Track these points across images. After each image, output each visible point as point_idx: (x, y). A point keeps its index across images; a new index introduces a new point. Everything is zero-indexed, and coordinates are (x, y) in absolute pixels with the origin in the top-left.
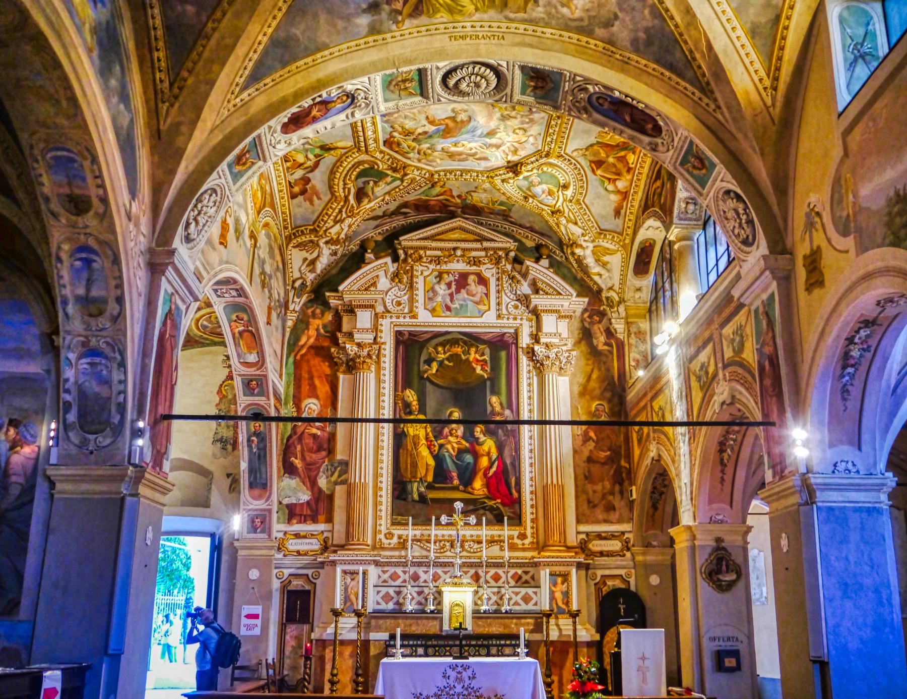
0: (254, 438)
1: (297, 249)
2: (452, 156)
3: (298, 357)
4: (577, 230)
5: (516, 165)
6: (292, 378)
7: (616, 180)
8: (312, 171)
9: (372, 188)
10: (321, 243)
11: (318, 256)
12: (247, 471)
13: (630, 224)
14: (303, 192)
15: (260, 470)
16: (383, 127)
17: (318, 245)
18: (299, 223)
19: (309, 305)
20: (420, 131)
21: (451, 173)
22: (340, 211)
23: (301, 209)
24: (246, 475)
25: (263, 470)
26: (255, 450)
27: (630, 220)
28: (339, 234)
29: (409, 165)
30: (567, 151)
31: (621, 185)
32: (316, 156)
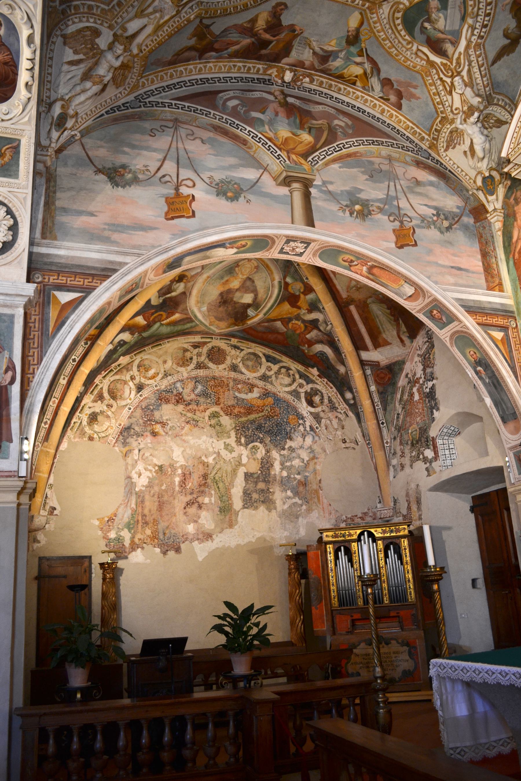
0: (479, 368)
1: (450, 149)
3: (517, 256)
6: (518, 282)
8: (379, 71)
9: (435, 29)
10: (458, 124)
11: (472, 140)
12: (493, 406)
14: (400, 95)
15: (502, 400)
17: (462, 131)
18: (428, 124)
19: (510, 194)
22: (441, 79)
24: (495, 410)
25: (505, 398)
26: (487, 381)
28: (463, 102)
32: (360, 54)
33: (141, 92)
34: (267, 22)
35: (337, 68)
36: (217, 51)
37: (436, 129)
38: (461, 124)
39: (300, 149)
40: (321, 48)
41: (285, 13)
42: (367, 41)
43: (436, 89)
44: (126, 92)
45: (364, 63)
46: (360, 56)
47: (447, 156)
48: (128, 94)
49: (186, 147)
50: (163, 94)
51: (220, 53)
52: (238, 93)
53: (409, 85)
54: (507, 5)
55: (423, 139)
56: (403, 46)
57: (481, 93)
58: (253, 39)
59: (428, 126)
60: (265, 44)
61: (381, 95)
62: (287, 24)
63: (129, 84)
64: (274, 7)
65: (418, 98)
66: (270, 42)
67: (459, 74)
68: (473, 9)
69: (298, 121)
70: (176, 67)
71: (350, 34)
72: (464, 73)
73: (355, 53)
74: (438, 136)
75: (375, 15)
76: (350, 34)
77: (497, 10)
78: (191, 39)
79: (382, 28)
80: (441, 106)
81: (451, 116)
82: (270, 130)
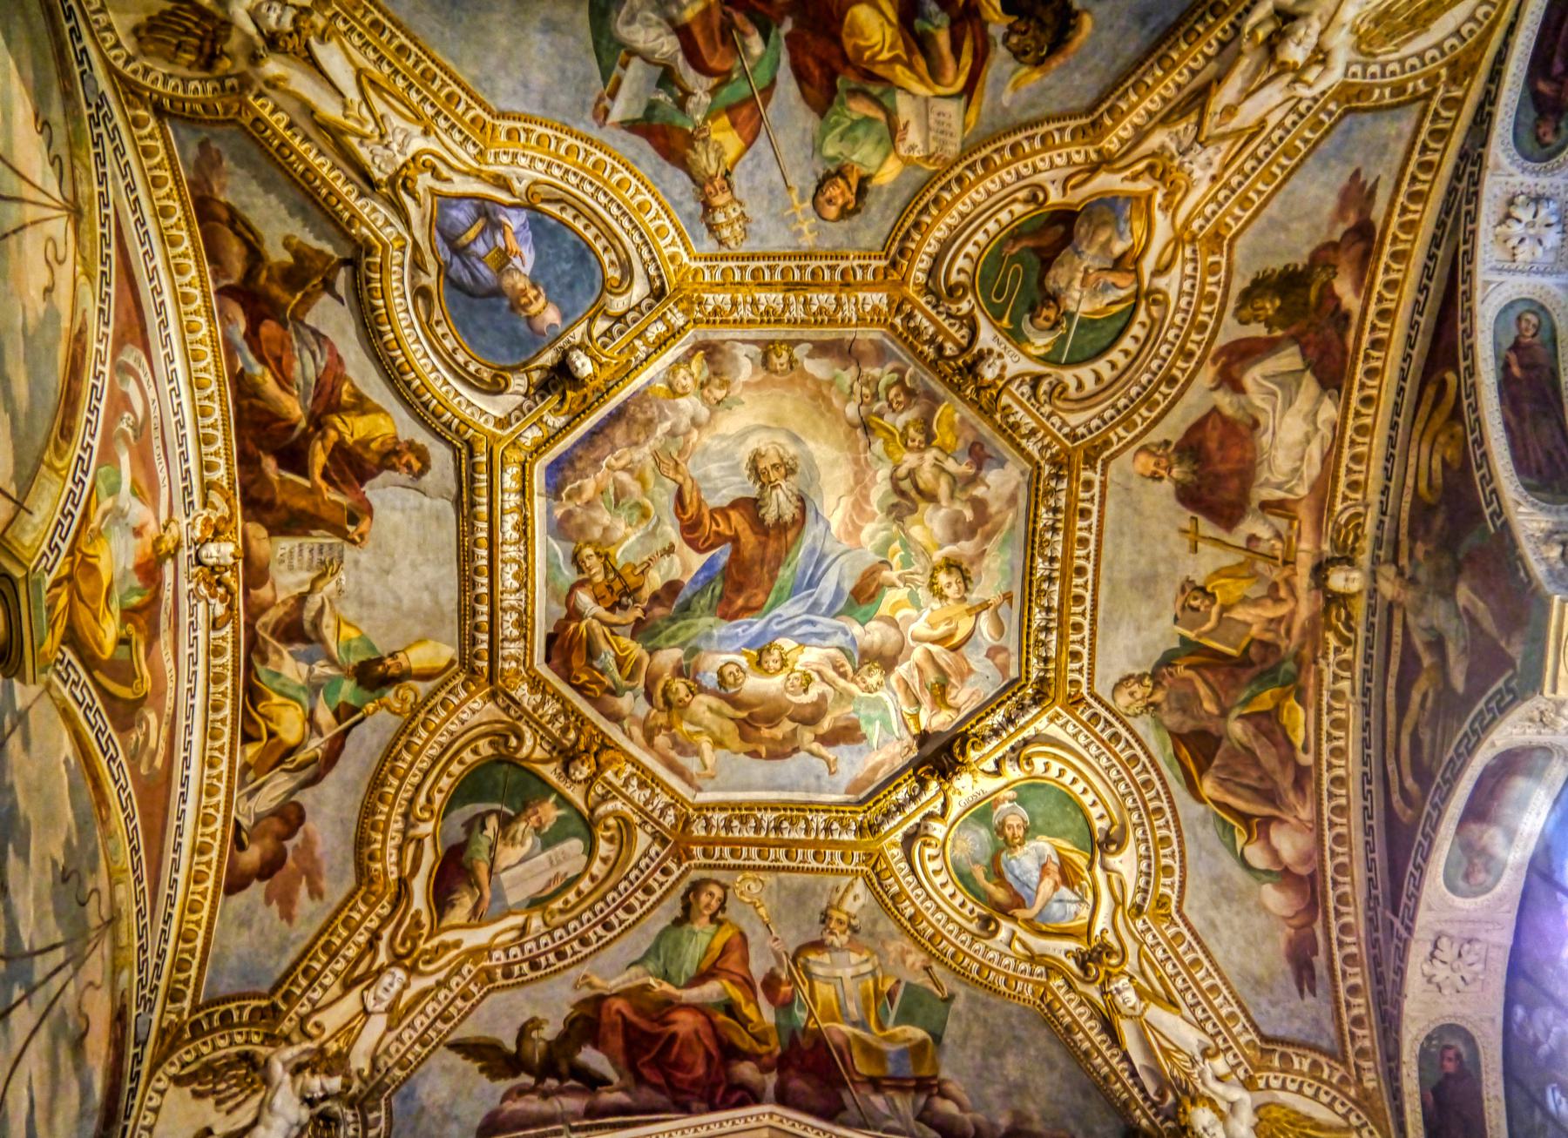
1: (187, 1090)
2: (754, 724)
4: (1180, 1031)
5: (947, 748)
7: (1267, 821)
9: (492, 848)
11: (255, 1123)
13: (1360, 1006)
14: (270, 868)
16: (551, 564)
17: (267, 1081)
20: (655, 580)
21: (744, 821)
22: (375, 936)
23: (251, 934)
27: (1353, 990)
29: (616, 747)
30: (1097, 690)
31: (1288, 844)
33: (118, 119)
34: (365, 443)
35: (278, 675)
36: (252, 335)
37: (228, 1013)
38: (285, 1064)
39: (84, 615)
40: (321, 611)
41: (403, 477)
42: (384, 711)
43: (345, 942)
44: (119, 64)
45: (321, 734)
46: (336, 714)
47: (162, 1093)
48: (111, 70)
49: (29, 230)
50: (122, 185)
51: (245, 346)
52: (155, 412)
53: (312, 875)
54: (590, 985)
55: (174, 996)
56: (411, 801)
57: (381, 1063)
58: (303, 424)
59: (223, 989)
60: (294, 459)
61: (245, 822)
62: (368, 495)
63: (147, 71)
64: (411, 446)
65: (287, 916)
66: (304, 472)
67: (412, 970)
68: (562, 911)
69: (135, 600)
70: (188, 223)
71: (389, 662)
72: (418, 984)
73: (341, 699)
74: (212, 1030)
75: (463, 695)
76: (389, 662)
77: (572, 972)
78: (287, 246)
79: (438, 727)
80: (304, 983)
81: (286, 1026)
82: (104, 515)
